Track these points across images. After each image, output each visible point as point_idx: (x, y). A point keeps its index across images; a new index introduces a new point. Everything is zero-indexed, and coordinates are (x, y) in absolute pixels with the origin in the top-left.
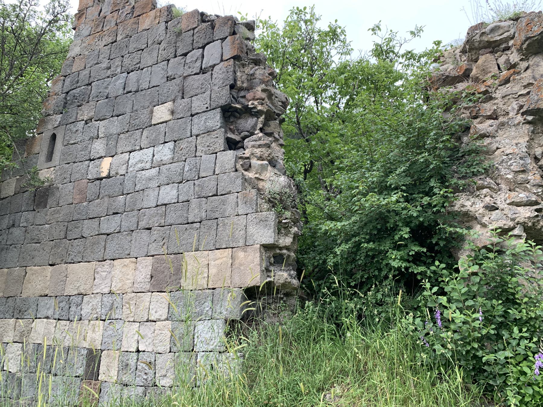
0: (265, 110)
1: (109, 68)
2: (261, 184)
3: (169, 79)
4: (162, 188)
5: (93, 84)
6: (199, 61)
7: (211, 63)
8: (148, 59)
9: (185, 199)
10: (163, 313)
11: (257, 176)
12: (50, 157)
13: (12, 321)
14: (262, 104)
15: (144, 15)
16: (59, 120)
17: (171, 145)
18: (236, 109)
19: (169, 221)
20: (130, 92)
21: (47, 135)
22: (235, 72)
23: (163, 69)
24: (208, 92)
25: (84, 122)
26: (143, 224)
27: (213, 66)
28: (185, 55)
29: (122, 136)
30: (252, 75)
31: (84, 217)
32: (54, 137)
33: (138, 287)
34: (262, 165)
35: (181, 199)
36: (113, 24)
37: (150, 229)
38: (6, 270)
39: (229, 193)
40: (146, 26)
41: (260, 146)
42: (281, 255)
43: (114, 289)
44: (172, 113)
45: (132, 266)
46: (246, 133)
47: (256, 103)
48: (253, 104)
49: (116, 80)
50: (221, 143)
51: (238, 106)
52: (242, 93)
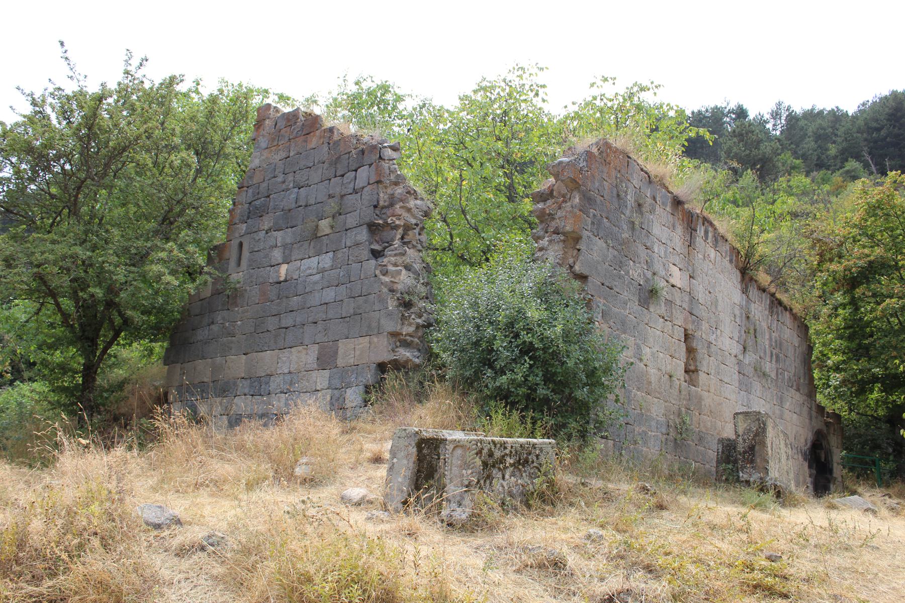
1: (284, 182)
2: (395, 287)
3: (331, 196)
4: (324, 290)
5: (271, 197)
6: (353, 183)
7: (361, 186)
8: (315, 176)
9: (341, 298)
10: (326, 384)
11: (392, 279)
12: (239, 264)
13: (218, 400)
14: (399, 219)
15: (312, 134)
16: (244, 229)
17: (331, 254)
18: (379, 224)
19: (330, 316)
20: (301, 206)
21: (235, 243)
24: (358, 211)
25: (264, 232)
26: (310, 319)
27: (363, 188)
28: (343, 176)
29: (295, 245)
32: (241, 245)
35: (338, 299)
36: (287, 139)
37: (316, 323)
38: (210, 360)
40: (313, 145)
41: (395, 255)
42: (405, 340)
43: (292, 370)
44: (332, 227)
45: (304, 352)
46: (386, 245)
47: (394, 219)
48: (392, 220)
49: (289, 195)
50: (366, 254)
51: (381, 222)
52: (384, 211)
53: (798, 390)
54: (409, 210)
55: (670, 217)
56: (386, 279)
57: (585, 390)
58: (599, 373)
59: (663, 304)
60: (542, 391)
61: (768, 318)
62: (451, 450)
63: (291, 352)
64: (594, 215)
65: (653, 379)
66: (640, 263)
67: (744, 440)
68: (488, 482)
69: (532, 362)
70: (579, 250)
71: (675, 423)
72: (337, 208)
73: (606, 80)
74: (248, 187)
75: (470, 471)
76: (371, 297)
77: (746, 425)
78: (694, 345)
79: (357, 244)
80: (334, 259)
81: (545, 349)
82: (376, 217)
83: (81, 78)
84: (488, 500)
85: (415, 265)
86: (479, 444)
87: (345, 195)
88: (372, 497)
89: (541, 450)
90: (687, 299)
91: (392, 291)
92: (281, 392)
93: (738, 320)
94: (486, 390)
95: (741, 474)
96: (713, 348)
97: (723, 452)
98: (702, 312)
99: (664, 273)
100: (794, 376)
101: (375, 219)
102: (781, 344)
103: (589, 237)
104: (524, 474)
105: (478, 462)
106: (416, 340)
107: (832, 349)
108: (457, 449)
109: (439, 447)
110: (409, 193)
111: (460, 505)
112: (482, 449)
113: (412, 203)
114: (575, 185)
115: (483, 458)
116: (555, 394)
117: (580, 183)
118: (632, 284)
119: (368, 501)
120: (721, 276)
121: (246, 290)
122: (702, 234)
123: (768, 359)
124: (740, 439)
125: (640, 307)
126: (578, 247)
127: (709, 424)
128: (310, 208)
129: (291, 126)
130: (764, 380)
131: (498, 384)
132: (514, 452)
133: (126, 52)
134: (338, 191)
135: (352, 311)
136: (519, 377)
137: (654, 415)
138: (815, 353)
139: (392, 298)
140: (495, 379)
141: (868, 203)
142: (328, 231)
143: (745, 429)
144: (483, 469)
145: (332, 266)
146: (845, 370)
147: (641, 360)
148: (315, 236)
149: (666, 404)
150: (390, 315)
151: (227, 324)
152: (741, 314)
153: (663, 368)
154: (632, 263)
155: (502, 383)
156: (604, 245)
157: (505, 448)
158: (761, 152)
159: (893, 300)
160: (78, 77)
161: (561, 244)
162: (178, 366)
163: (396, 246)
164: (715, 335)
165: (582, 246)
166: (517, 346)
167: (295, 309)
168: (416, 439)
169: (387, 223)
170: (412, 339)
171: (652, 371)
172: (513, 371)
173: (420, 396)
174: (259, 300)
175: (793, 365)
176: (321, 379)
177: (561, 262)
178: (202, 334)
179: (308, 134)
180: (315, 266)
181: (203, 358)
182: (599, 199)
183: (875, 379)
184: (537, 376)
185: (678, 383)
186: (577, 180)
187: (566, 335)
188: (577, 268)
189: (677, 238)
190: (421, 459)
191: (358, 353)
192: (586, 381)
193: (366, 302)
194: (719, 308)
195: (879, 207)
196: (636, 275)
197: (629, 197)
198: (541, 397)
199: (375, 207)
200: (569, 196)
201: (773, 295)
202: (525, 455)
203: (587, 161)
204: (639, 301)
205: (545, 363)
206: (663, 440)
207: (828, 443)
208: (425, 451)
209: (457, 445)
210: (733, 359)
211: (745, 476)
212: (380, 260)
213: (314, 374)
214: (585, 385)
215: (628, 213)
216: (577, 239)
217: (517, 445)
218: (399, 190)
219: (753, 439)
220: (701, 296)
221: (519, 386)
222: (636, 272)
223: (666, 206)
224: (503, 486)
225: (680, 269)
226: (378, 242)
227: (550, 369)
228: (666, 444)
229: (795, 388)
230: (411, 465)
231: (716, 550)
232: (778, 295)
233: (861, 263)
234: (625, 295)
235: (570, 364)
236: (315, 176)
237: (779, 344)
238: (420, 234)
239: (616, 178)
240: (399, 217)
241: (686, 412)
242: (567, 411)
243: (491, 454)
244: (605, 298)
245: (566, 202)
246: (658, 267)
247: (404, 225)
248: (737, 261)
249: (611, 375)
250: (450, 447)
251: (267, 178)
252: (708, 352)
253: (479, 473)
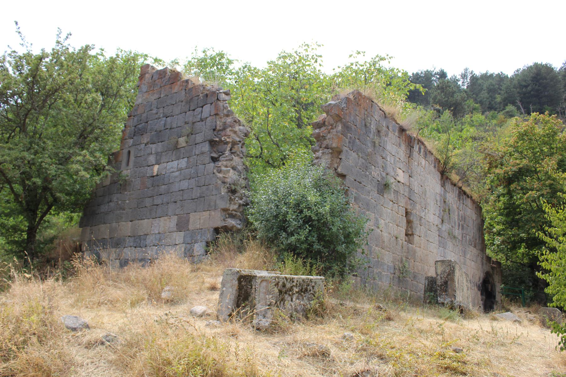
0: (231, 141)
1: (157, 113)
2: (226, 180)
3: (186, 123)
4: (181, 182)
5: (149, 122)
6: (200, 115)
7: (205, 117)
8: (177, 110)
9: (192, 187)
11: (224, 176)
12: (128, 164)
13: (114, 250)
14: (229, 138)
15: (175, 84)
16: (132, 142)
17: (186, 159)
18: (216, 141)
19: (185, 198)
21: (125, 151)
22: (216, 122)
23: (183, 117)
24: (203, 132)
25: (144, 145)
26: (172, 200)
27: (207, 118)
28: (194, 110)
29: (163, 153)
30: (225, 122)
31: (146, 196)
33: (171, 230)
34: (226, 170)
35: (190, 187)
36: (159, 86)
37: (176, 202)
38: (109, 225)
39: (210, 184)
40: (175, 91)
41: (226, 160)
42: (232, 214)
43: (160, 231)
44: (187, 142)
46: (221, 154)
47: (226, 138)
48: (224, 138)
49: (160, 121)
50: (208, 159)
51: (217, 139)
52: (220, 132)
53: (475, 247)
54: (235, 132)
55: (398, 139)
56: (221, 175)
57: (343, 246)
58: (352, 235)
59: (392, 193)
60: (316, 247)
61: (457, 202)
62: (259, 283)
63: (160, 220)
64: (350, 137)
65: (386, 240)
66: (378, 167)
67: (441, 278)
68: (282, 303)
69: (310, 229)
70: (341, 159)
71: (399, 267)
72: (190, 130)
73: (359, 53)
74: (134, 116)
75: (271, 296)
76: (211, 187)
77: (442, 269)
78: (411, 218)
79: (203, 153)
80: (188, 162)
81: (318, 220)
82: (214, 136)
83: (29, 45)
84: (282, 314)
85: (238, 167)
86: (277, 279)
87: (195, 122)
88: (209, 311)
89: (315, 283)
90: (407, 190)
91: (224, 183)
92: (154, 245)
93: (439, 203)
94: (281, 246)
95: (439, 299)
96: (423, 221)
97: (428, 285)
98: (416, 198)
99: (393, 174)
100: (473, 238)
101: (214, 138)
102: (465, 218)
103: (347, 151)
104: (305, 298)
105: (276, 290)
106: (239, 214)
107: (496, 221)
108: (263, 282)
109: (252, 281)
110: (235, 121)
111: (265, 317)
112: (279, 282)
113: (237, 128)
114: (339, 118)
115: (279, 288)
116: (325, 248)
117: (342, 117)
118: (373, 181)
119: (207, 314)
120: (429, 176)
121: (132, 181)
122: (417, 150)
123: (457, 227)
124: (439, 277)
125: (378, 195)
126: (340, 157)
127: (420, 267)
128: (173, 130)
129: (162, 78)
130: (454, 241)
131: (289, 242)
132: (298, 284)
133: (57, 29)
134: (191, 119)
135: (198, 195)
136: (303, 238)
137: (386, 262)
138: (486, 224)
139: (223, 187)
140: (288, 239)
141: (519, 132)
142: (184, 144)
143: (442, 271)
144: (279, 295)
145: (187, 167)
146: (503, 235)
147: (378, 227)
148: (176, 147)
149: (394, 255)
150: (222, 198)
151: (120, 202)
152: (441, 200)
153: (392, 233)
154: (373, 167)
155: (292, 241)
156: (356, 156)
157: (293, 282)
158: (454, 99)
159: (533, 192)
160: (27, 44)
161: (330, 155)
162: (89, 228)
163: (227, 154)
164: (424, 212)
165: (343, 156)
166: (301, 218)
167: (163, 193)
168: (238, 275)
169: (221, 140)
170: (236, 213)
171: (385, 234)
172: (299, 234)
173: (241, 249)
174: (140, 187)
175: (472, 231)
176: (179, 237)
177: (329, 166)
178: (104, 208)
179: (172, 84)
180: (176, 166)
181: (105, 223)
182: (353, 127)
183: (522, 240)
184: (313, 237)
185: (401, 242)
186: (340, 115)
187: (332, 212)
188: (339, 170)
189: (402, 152)
190: (240, 288)
191: (202, 221)
192: (344, 240)
193: (207, 189)
194: (427, 196)
195: (525, 134)
196: (376, 175)
197: (372, 126)
198: (316, 250)
199: (214, 130)
200: (335, 125)
201: (460, 188)
202: (305, 286)
203: (346, 104)
204: (378, 191)
205: (319, 229)
206: (392, 277)
207: (493, 280)
208: (243, 283)
209: (263, 279)
210: (435, 227)
211: (441, 300)
212: (217, 163)
213: (175, 234)
214: (343, 243)
215: (371, 136)
216: (340, 152)
217: (300, 280)
218: (229, 120)
219: (446, 277)
220: (416, 188)
221: (303, 243)
222: (376, 173)
223: (395, 132)
224: (291, 306)
225: (403, 172)
226: (215, 152)
227: (321, 233)
228: (393, 280)
229: (473, 245)
230: (234, 292)
231: (423, 345)
232: (463, 188)
233: (514, 169)
234: (369, 187)
235: (334, 229)
236: (177, 110)
237: (464, 219)
238: (242, 147)
239: (364, 114)
240: (229, 136)
241: (406, 260)
242: (332, 259)
243: (284, 286)
244: (356, 189)
245: (333, 129)
246: (390, 170)
247: (232, 141)
248: (439, 167)
249: (360, 237)
250: (259, 281)
251: (146, 111)
252: (420, 223)
253: (277, 297)
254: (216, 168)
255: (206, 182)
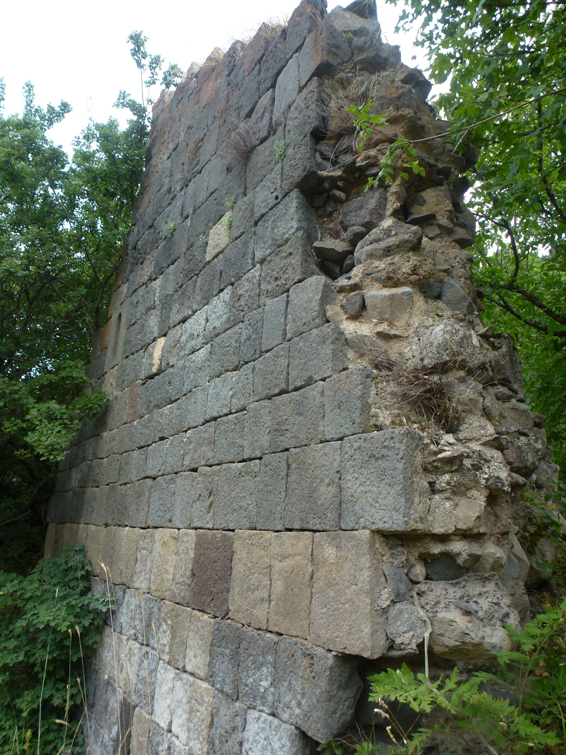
11: (383, 327)
34: (392, 297)
39: (310, 382)
41: (388, 251)
42: (449, 557)
170: (476, 549)
254: (341, 297)
255: (293, 373)
